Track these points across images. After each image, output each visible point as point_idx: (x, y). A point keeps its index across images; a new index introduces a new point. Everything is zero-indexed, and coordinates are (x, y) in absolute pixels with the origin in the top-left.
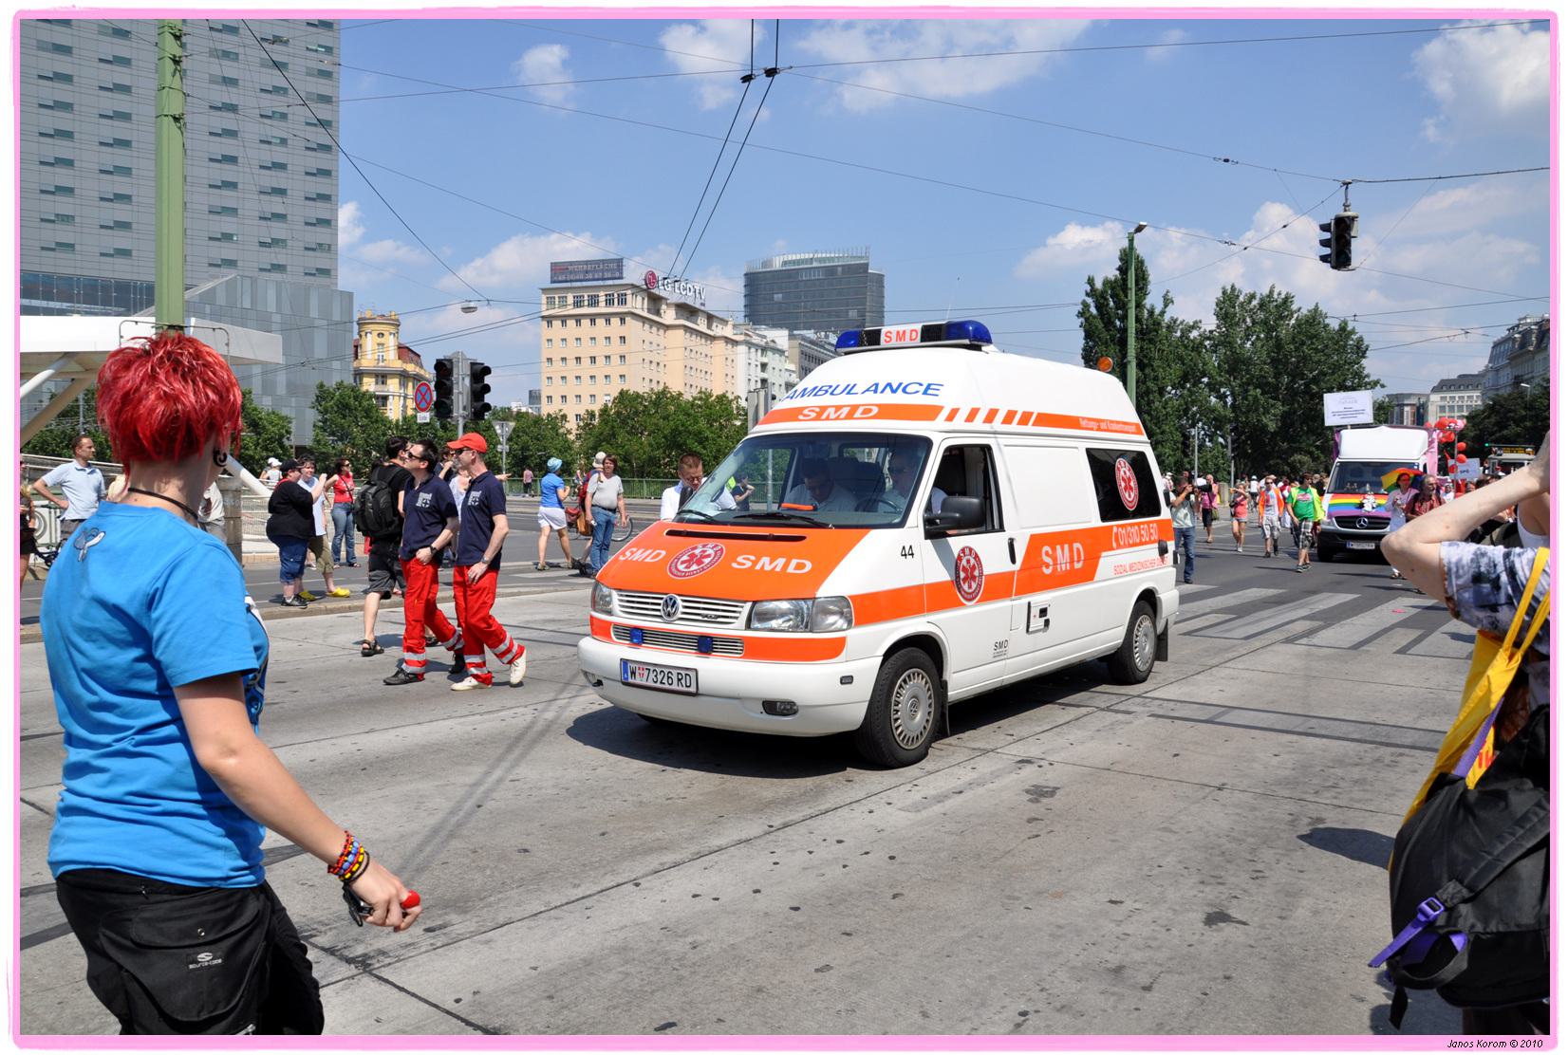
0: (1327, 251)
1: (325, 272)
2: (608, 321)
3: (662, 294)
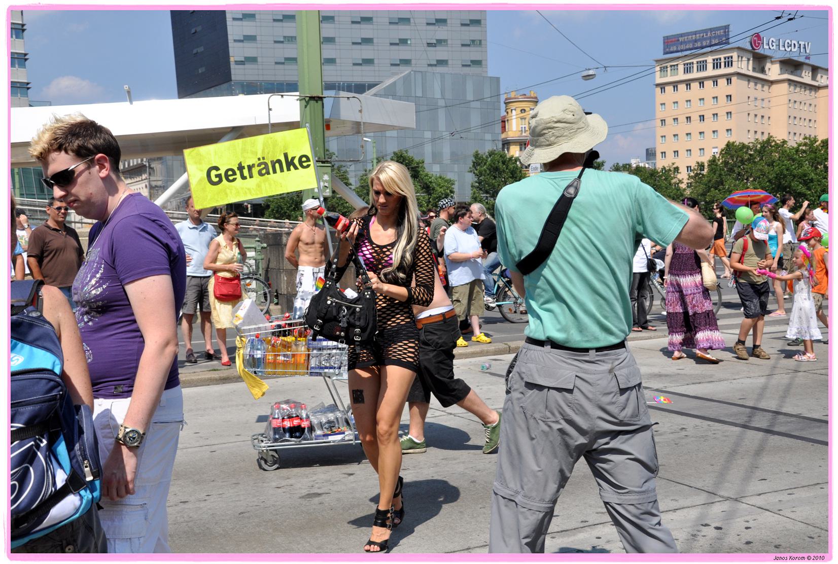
1: (477, 63)
2: (716, 83)
3: (767, 53)
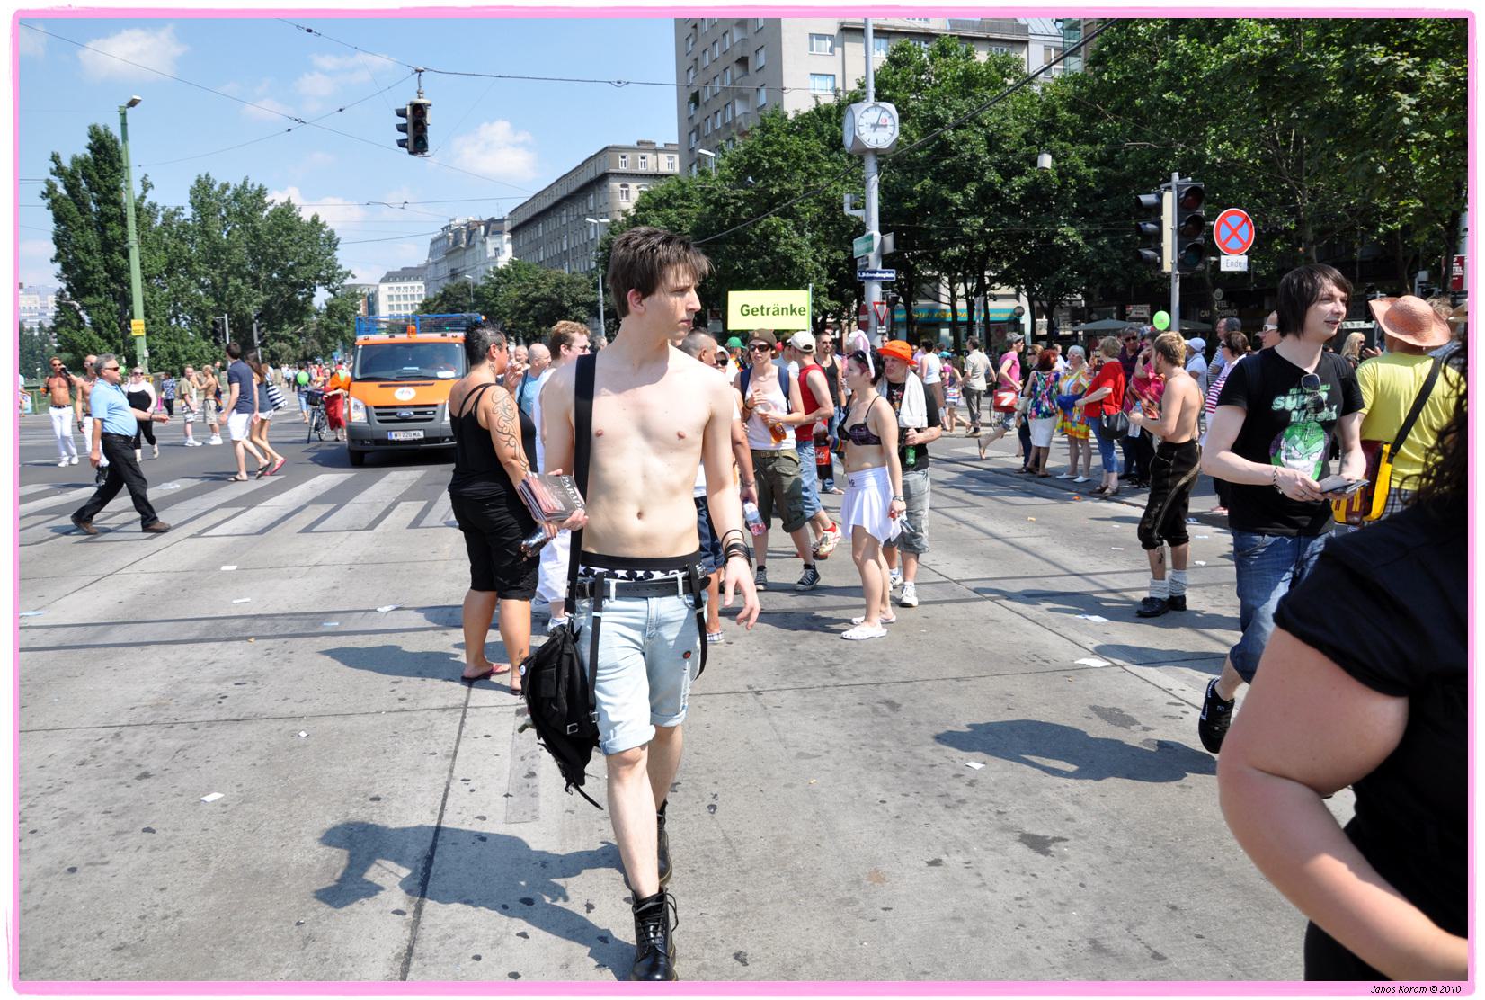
0: (404, 136)
